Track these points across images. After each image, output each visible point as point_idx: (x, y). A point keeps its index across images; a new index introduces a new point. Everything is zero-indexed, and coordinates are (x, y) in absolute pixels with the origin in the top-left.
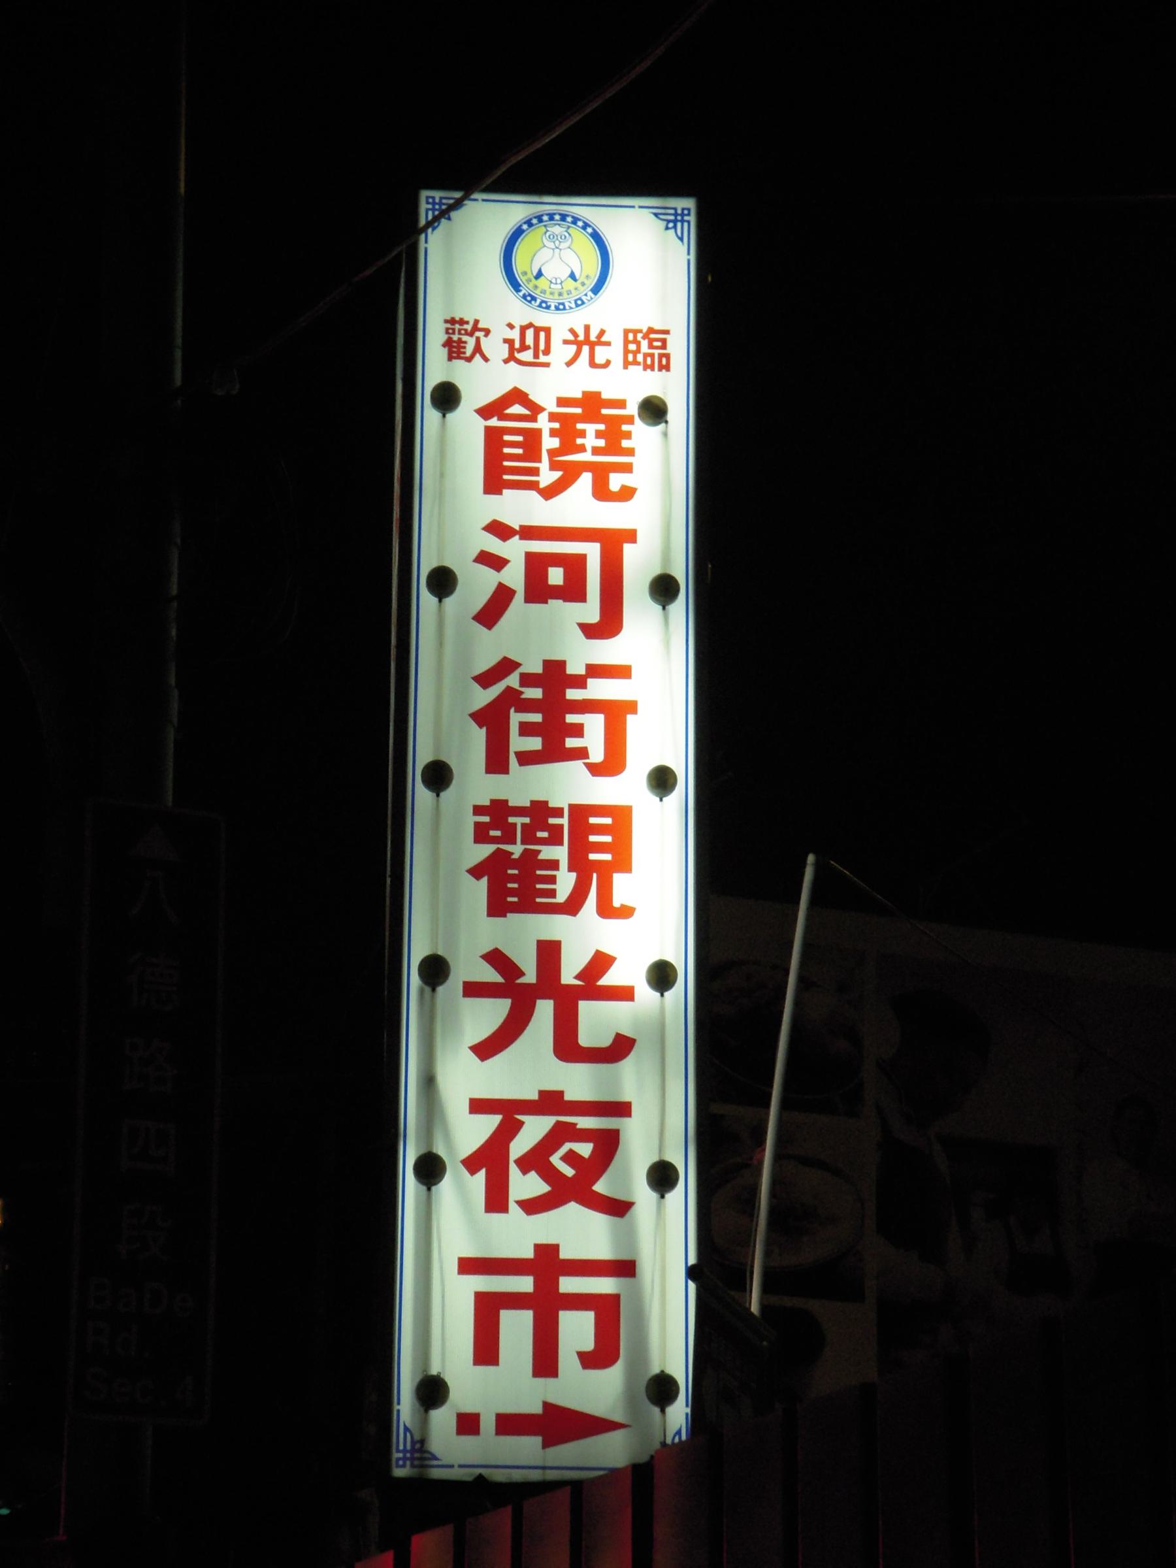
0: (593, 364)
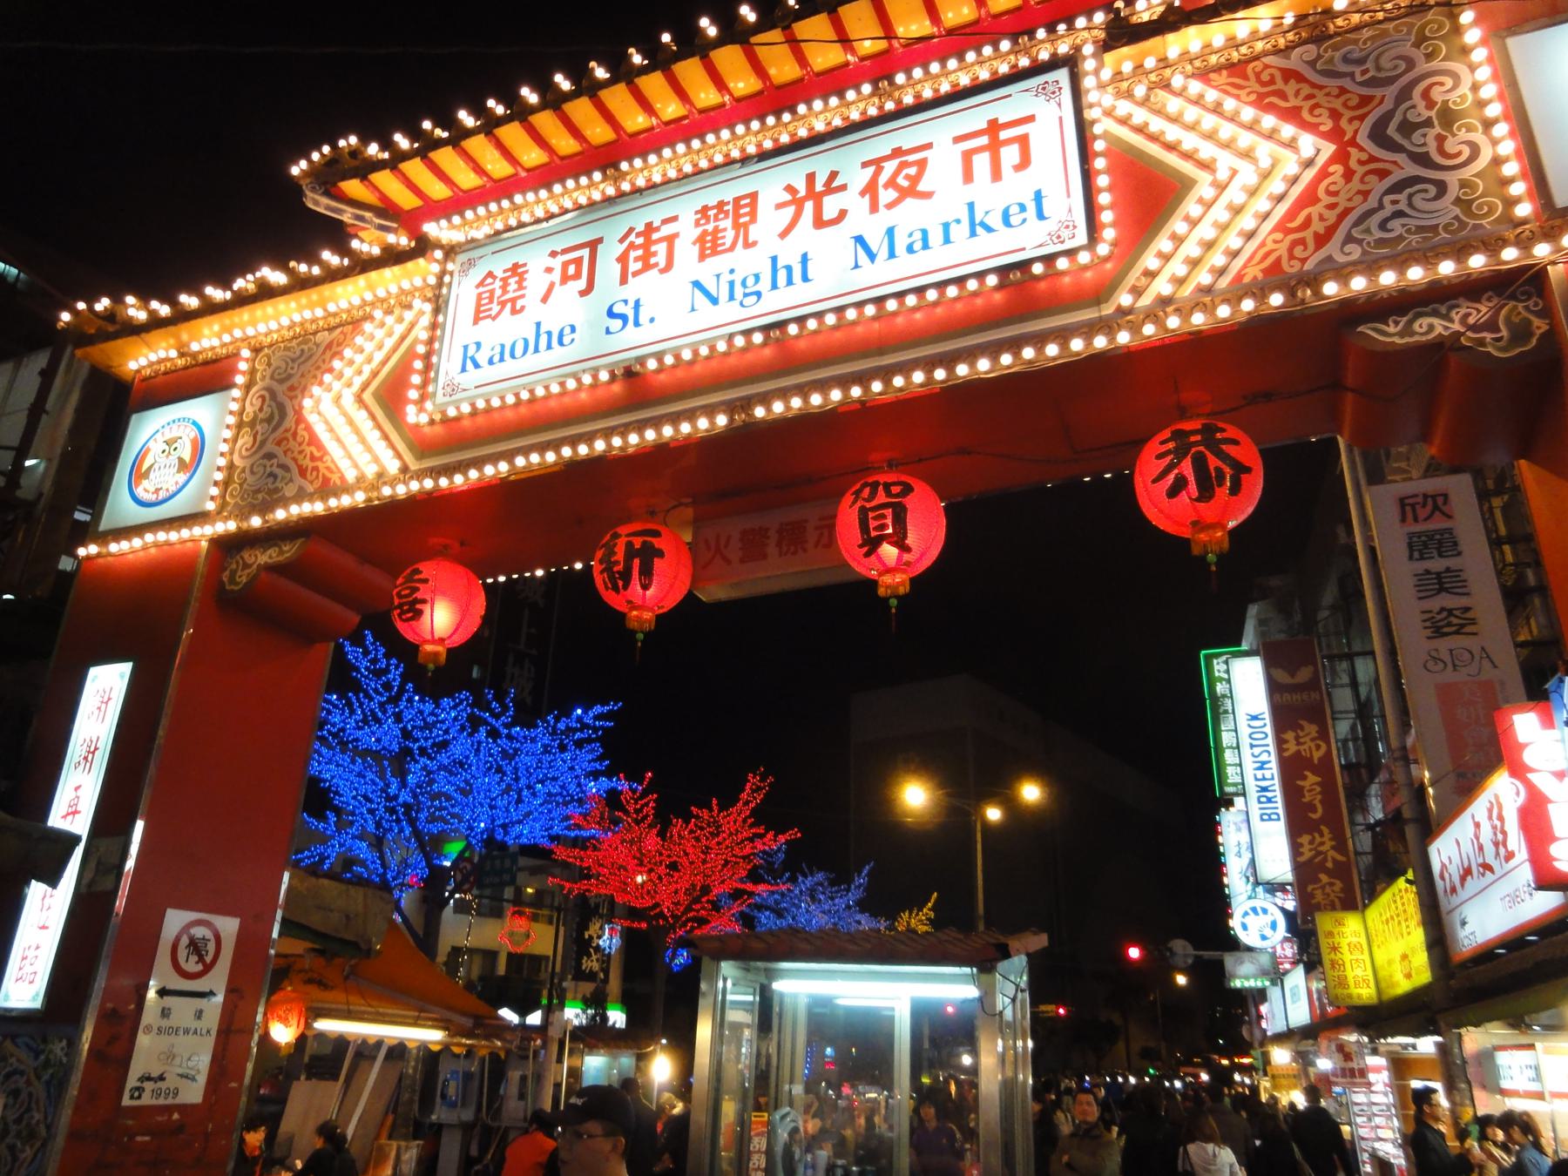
0: (819, 223)
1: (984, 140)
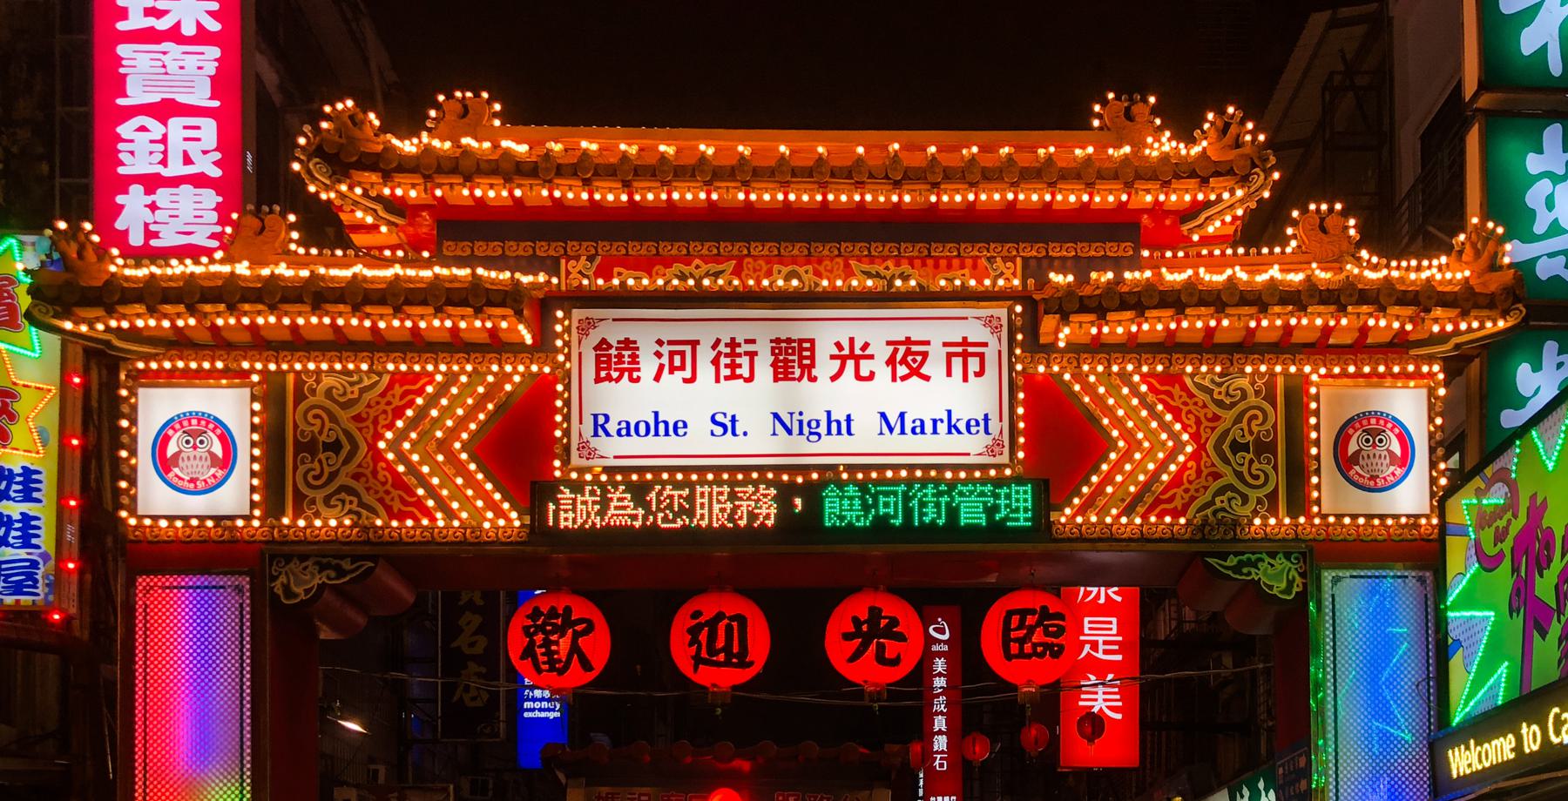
0: (858, 377)
1: (959, 349)
